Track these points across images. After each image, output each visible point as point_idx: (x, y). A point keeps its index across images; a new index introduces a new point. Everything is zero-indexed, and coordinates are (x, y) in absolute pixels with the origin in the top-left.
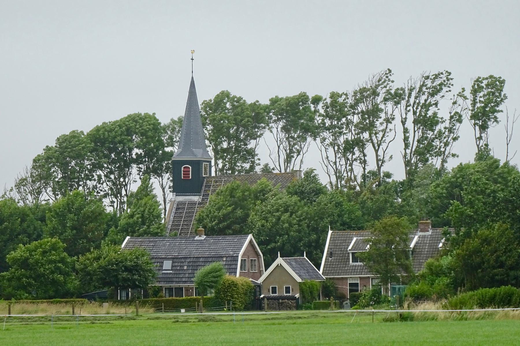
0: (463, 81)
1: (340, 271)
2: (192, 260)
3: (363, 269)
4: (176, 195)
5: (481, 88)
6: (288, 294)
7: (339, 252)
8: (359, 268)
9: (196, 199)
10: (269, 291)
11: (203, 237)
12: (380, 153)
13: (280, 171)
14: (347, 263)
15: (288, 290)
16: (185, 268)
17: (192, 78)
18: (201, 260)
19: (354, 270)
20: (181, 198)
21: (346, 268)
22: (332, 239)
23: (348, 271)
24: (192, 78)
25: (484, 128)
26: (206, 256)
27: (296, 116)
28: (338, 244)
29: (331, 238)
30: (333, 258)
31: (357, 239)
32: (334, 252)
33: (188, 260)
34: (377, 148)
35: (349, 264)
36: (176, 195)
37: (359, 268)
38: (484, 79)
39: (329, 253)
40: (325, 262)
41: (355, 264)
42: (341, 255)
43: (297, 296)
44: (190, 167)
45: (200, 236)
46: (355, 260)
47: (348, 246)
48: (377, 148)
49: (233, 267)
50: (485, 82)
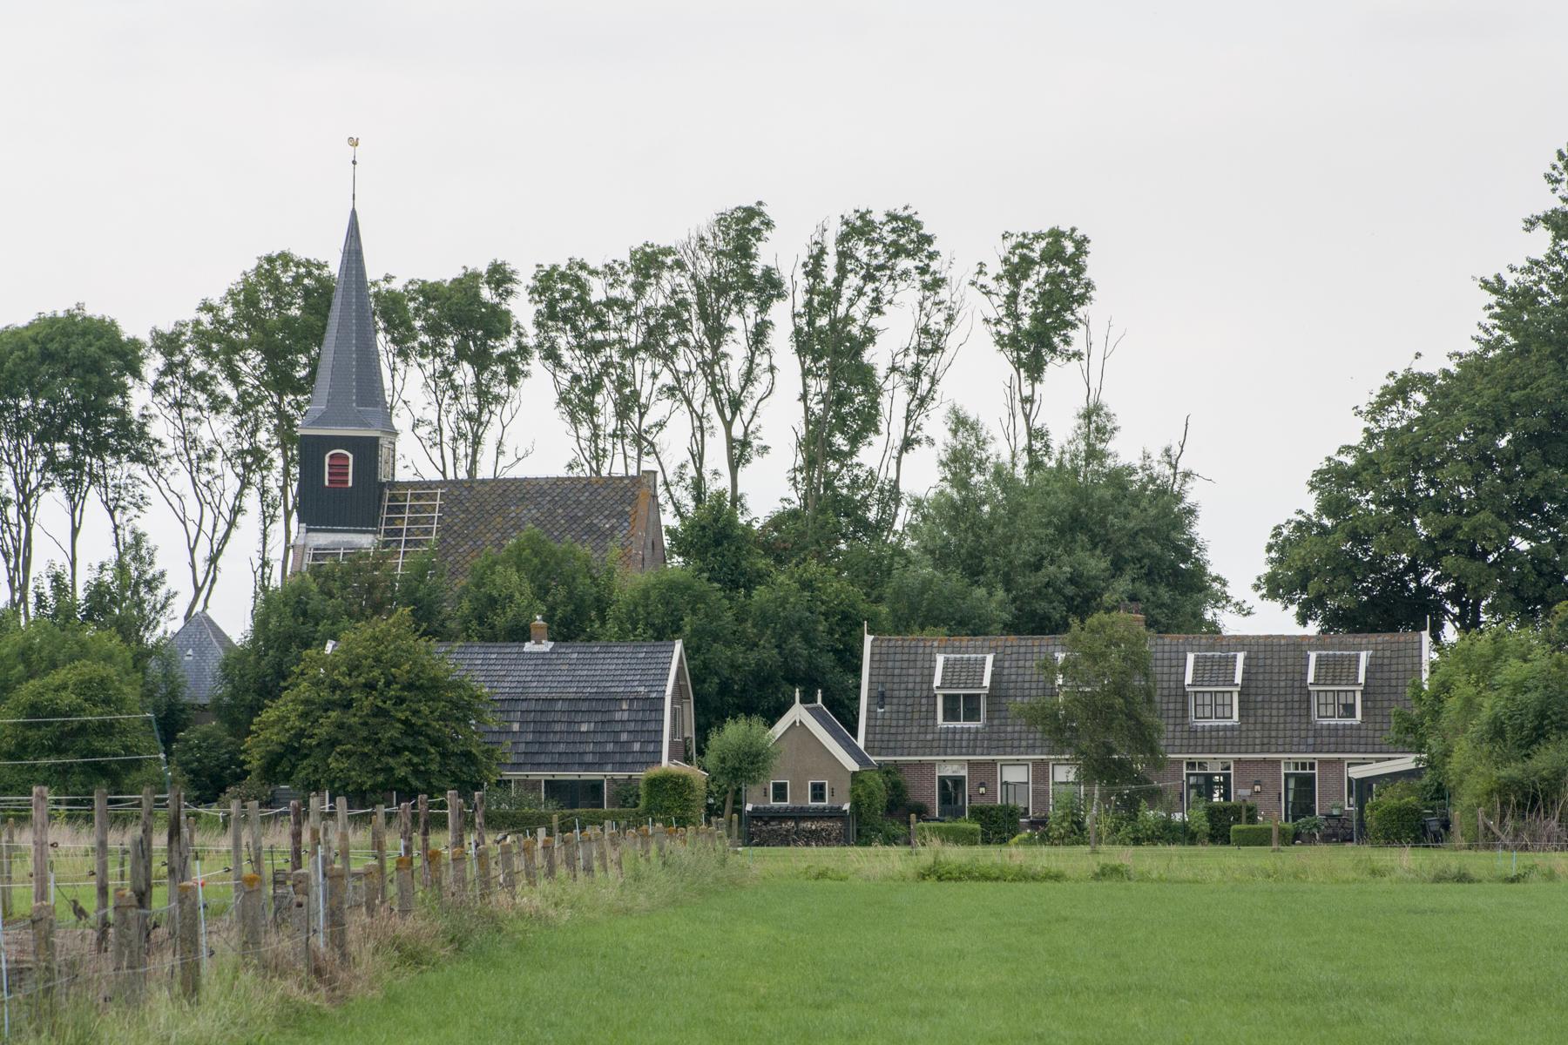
0: (970, 246)
1: (914, 744)
2: (532, 706)
3: (975, 740)
4: (308, 531)
5: (1026, 265)
6: (821, 804)
7: (903, 693)
8: (965, 736)
9: (365, 541)
10: (766, 794)
11: (547, 646)
12: (737, 432)
13: (444, 473)
14: (930, 722)
15: (818, 793)
16: (516, 727)
17: (354, 213)
18: (559, 706)
19: (949, 744)
20: (322, 539)
21: (929, 737)
22: (877, 657)
23: (935, 744)
24: (354, 213)
25: (1034, 369)
26: (572, 696)
27: (463, 320)
28: (897, 672)
29: (872, 654)
30: (887, 708)
31: (947, 660)
32: (888, 693)
33: (524, 706)
34: (728, 416)
35: (935, 725)
36: (308, 531)
37: (965, 736)
38: (1038, 237)
39: (874, 693)
40: (868, 718)
41: (952, 725)
42: (909, 701)
43: (846, 807)
44: (351, 456)
45: (538, 642)
46: (951, 714)
47: (932, 675)
48: (728, 416)
49: (652, 726)
50: (1040, 246)
